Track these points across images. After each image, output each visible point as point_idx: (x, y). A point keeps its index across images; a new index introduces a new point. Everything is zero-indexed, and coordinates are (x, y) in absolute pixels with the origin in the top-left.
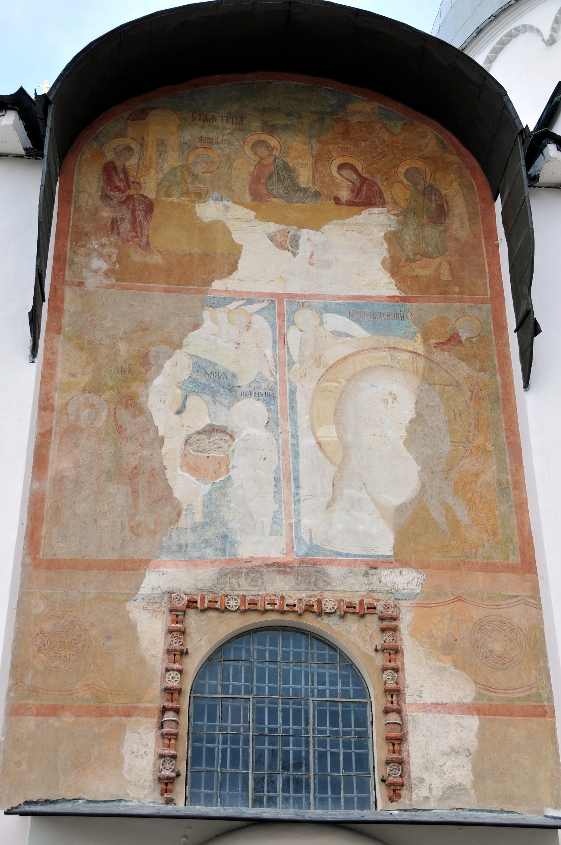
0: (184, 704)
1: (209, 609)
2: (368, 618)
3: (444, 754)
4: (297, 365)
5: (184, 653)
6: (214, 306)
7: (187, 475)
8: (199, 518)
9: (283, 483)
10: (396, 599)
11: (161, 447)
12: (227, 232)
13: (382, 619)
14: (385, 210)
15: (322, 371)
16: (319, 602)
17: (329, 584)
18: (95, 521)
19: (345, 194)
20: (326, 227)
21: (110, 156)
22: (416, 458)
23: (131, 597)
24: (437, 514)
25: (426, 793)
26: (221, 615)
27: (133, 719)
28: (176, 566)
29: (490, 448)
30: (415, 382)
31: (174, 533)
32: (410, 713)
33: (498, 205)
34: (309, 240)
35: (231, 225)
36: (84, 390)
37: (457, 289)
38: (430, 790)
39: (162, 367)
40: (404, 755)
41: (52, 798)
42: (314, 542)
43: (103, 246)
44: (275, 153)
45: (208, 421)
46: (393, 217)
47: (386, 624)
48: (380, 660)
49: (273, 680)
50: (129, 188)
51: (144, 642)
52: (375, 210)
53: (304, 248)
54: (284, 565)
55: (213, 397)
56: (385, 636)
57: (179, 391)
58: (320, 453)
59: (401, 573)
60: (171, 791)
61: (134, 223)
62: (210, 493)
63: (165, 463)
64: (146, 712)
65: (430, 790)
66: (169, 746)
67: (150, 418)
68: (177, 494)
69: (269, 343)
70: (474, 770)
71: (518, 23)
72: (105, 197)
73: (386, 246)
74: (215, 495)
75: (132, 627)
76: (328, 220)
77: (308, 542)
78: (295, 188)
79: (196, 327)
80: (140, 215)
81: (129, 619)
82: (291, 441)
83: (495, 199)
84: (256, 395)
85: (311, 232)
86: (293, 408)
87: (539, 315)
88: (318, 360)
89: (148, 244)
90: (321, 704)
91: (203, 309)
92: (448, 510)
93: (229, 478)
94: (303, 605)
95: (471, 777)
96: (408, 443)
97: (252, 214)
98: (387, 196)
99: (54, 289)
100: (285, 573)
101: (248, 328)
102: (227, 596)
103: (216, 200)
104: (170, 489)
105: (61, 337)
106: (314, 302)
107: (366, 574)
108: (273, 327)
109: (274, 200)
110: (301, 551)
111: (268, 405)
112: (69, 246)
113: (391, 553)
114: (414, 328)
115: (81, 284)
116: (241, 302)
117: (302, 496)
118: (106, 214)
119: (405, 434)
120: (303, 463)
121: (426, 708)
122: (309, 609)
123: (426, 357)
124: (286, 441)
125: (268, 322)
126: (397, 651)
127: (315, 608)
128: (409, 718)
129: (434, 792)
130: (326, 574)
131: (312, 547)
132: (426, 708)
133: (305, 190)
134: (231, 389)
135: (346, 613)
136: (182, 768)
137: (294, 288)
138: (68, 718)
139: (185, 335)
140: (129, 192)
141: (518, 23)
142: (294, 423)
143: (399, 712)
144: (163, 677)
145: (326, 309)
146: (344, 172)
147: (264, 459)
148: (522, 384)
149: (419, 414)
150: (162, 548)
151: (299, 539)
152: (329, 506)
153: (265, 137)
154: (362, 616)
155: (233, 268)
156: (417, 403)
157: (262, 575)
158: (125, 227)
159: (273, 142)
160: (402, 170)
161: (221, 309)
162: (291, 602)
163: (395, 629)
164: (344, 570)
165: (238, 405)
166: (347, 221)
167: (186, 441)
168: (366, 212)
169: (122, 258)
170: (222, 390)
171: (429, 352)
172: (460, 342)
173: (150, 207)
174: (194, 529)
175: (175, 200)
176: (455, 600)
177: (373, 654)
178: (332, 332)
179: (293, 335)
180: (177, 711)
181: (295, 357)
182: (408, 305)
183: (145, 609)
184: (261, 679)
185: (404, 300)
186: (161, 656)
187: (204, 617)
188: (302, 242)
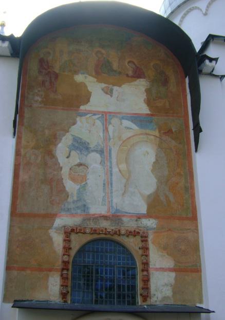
0: (70, 267)
1: (79, 232)
2: (137, 237)
3: (163, 286)
4: (112, 140)
5: (70, 249)
6: (81, 116)
7: (71, 182)
8: (75, 198)
9: (106, 186)
10: (147, 230)
11: (61, 171)
12: (86, 87)
13: (142, 237)
14: (145, 80)
15: (121, 142)
16: (119, 231)
17: (123, 224)
18: (37, 199)
19: (130, 73)
20: (123, 86)
21: (42, 56)
22: (156, 177)
23: (50, 228)
24: (162, 198)
25: (156, 299)
26: (83, 235)
27: (52, 273)
28: (67, 216)
29: (183, 174)
31: (66, 204)
32: (151, 271)
33: (187, 80)
34: (117, 91)
35: (87, 84)
36: (32, 148)
37: (171, 112)
38: (157, 298)
39: (61, 139)
40: (149, 286)
41: (24, 299)
42: (118, 208)
43: (39, 91)
44: (104, 56)
45: (78, 161)
46: (148, 83)
47: (143, 239)
48: (141, 252)
49: (102, 259)
50: (49, 68)
51: (55, 245)
52: (142, 80)
53: (115, 93)
54: (106, 217)
55: (81, 151)
56: (143, 244)
57: (68, 149)
58: (120, 174)
59: (149, 220)
60: (66, 298)
61: (51, 83)
62: (79, 189)
63: (63, 177)
64: (57, 270)
65: (157, 298)
66: (65, 282)
67: (57, 160)
68: (67, 189)
69: (102, 130)
70: (173, 291)
71: (193, 6)
72: (40, 72)
73: (145, 94)
74: (81, 190)
75: (51, 239)
76: (124, 83)
77: (115, 208)
79: (74, 124)
80: (53, 80)
81: (50, 236)
82: (109, 170)
83: (186, 77)
84: (96, 151)
85: (118, 88)
86: (110, 156)
87: (202, 125)
88: (120, 138)
89: (56, 91)
90: (119, 267)
91: (77, 117)
92: (167, 197)
93: (86, 183)
94: (113, 232)
95: (172, 294)
96: (152, 171)
97: (95, 80)
99: (21, 108)
100: (107, 220)
101: (94, 125)
102: (85, 228)
103: (82, 74)
104: (65, 187)
105: (24, 127)
106: (118, 115)
107: (137, 221)
108: (103, 124)
109: (103, 74)
110: (112, 211)
111: (101, 155)
112: (26, 91)
113: (146, 213)
114: (155, 127)
115: (31, 106)
116: (91, 115)
117: (113, 191)
118: (40, 78)
119: (151, 167)
120: (114, 178)
121: (157, 269)
122: (115, 233)
123: (160, 138)
124: (107, 169)
125: (101, 122)
126: (147, 249)
127: (118, 233)
128: (151, 273)
129: (159, 299)
130: (122, 220)
131: (117, 210)
132: (157, 269)
133: (115, 71)
134: (87, 149)
135: (129, 235)
136: (69, 289)
138: (28, 272)
139: (70, 127)
140: (49, 70)
141: (194, 5)
142: (111, 162)
143: (147, 271)
144: (62, 258)
145: (123, 118)
146: (130, 64)
147: (100, 176)
148: (194, 150)
149: (157, 160)
150: (62, 209)
151: (112, 207)
152: (123, 194)
154: (135, 236)
155: (88, 101)
156: (156, 156)
157: (98, 220)
158: (47, 84)
159: (103, 51)
160: (152, 64)
161: (84, 117)
162: (109, 230)
163: (147, 241)
164: (128, 219)
165: (90, 155)
166: (131, 84)
167: (70, 169)
168: (138, 80)
170: (84, 149)
171: (160, 136)
172: (172, 132)
173: (57, 76)
174: (74, 202)
175: (66, 73)
176: (168, 231)
177: (138, 250)
178: (125, 127)
179: (111, 128)
180: (68, 270)
181: (111, 137)
182: (153, 117)
183: (55, 232)
184: (97, 258)
185: (152, 115)
186: (61, 250)
187: (77, 235)
188: (114, 92)
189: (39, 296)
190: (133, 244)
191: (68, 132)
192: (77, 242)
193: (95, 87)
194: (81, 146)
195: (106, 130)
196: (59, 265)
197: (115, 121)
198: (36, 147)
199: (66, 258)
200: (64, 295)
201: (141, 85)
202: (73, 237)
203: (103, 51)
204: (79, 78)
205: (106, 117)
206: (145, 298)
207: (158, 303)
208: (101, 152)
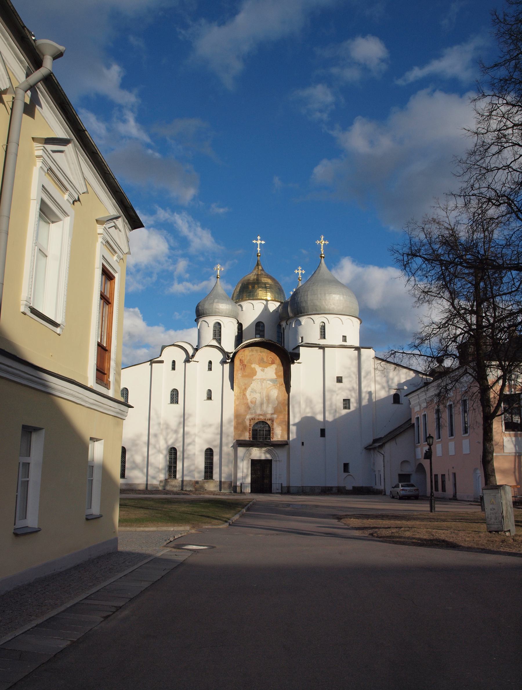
0: (251, 430)
12: (255, 369)
19: (270, 362)
20: (268, 368)
30: (278, 390)
53: (265, 371)
61: (244, 368)
72: (240, 365)
75: (245, 422)
78: (264, 362)
84: (259, 393)
97: (258, 366)
98: (276, 362)
110: (264, 413)
115: (238, 378)
118: (240, 367)
134: (256, 392)
137: (264, 377)
145: (268, 380)
153: (260, 353)
155: (256, 375)
159: (261, 354)
169: (243, 374)
173: (246, 366)
179: (263, 384)
189: (242, 438)
190: (269, 422)
191: (249, 386)
192: (253, 423)
193: (258, 369)
194: (253, 391)
195: (262, 385)
196: (248, 430)
197: (265, 381)
198: (240, 393)
199: (250, 427)
200: (250, 438)
201: (274, 366)
202: (252, 421)
203: (261, 354)
204: (253, 366)
205: (262, 380)
206: (272, 439)
207: (276, 440)
208: (260, 393)
